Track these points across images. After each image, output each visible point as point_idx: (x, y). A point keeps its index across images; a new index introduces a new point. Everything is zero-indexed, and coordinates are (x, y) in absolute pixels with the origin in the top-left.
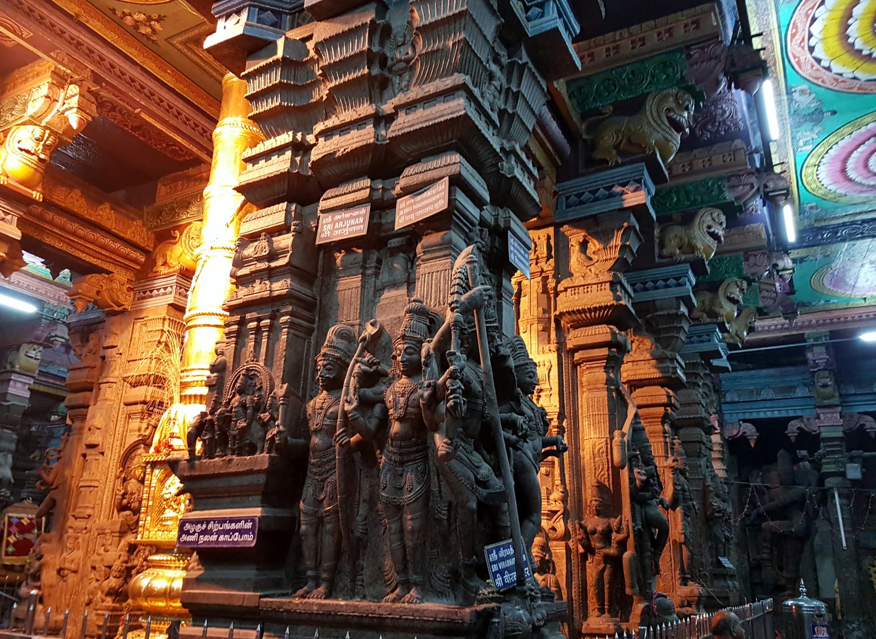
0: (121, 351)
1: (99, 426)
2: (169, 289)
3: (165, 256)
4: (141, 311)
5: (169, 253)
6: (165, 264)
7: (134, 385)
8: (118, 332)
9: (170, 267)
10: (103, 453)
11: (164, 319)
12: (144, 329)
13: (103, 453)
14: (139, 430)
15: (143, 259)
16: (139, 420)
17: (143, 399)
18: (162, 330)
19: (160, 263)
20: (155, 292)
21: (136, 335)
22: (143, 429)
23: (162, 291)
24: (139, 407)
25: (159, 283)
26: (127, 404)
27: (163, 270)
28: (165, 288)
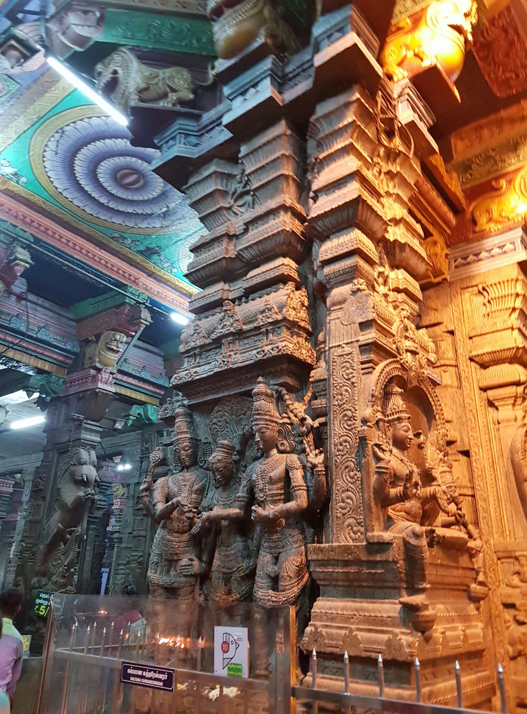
0: (451, 328)
1: (449, 418)
2: (509, 247)
3: (488, 211)
4: (470, 278)
5: (495, 208)
6: (490, 220)
7: (484, 366)
8: (440, 307)
9: (500, 223)
10: (466, 453)
11: (517, 280)
12: (480, 299)
13: (466, 453)
14: (516, 419)
15: (454, 222)
16: (510, 407)
17: (516, 379)
18: (517, 295)
19: (482, 220)
20: (484, 254)
21: (467, 307)
22: (519, 418)
23: (496, 251)
24: (511, 390)
25: (488, 243)
26: (484, 389)
27: (492, 226)
28: (501, 247)
